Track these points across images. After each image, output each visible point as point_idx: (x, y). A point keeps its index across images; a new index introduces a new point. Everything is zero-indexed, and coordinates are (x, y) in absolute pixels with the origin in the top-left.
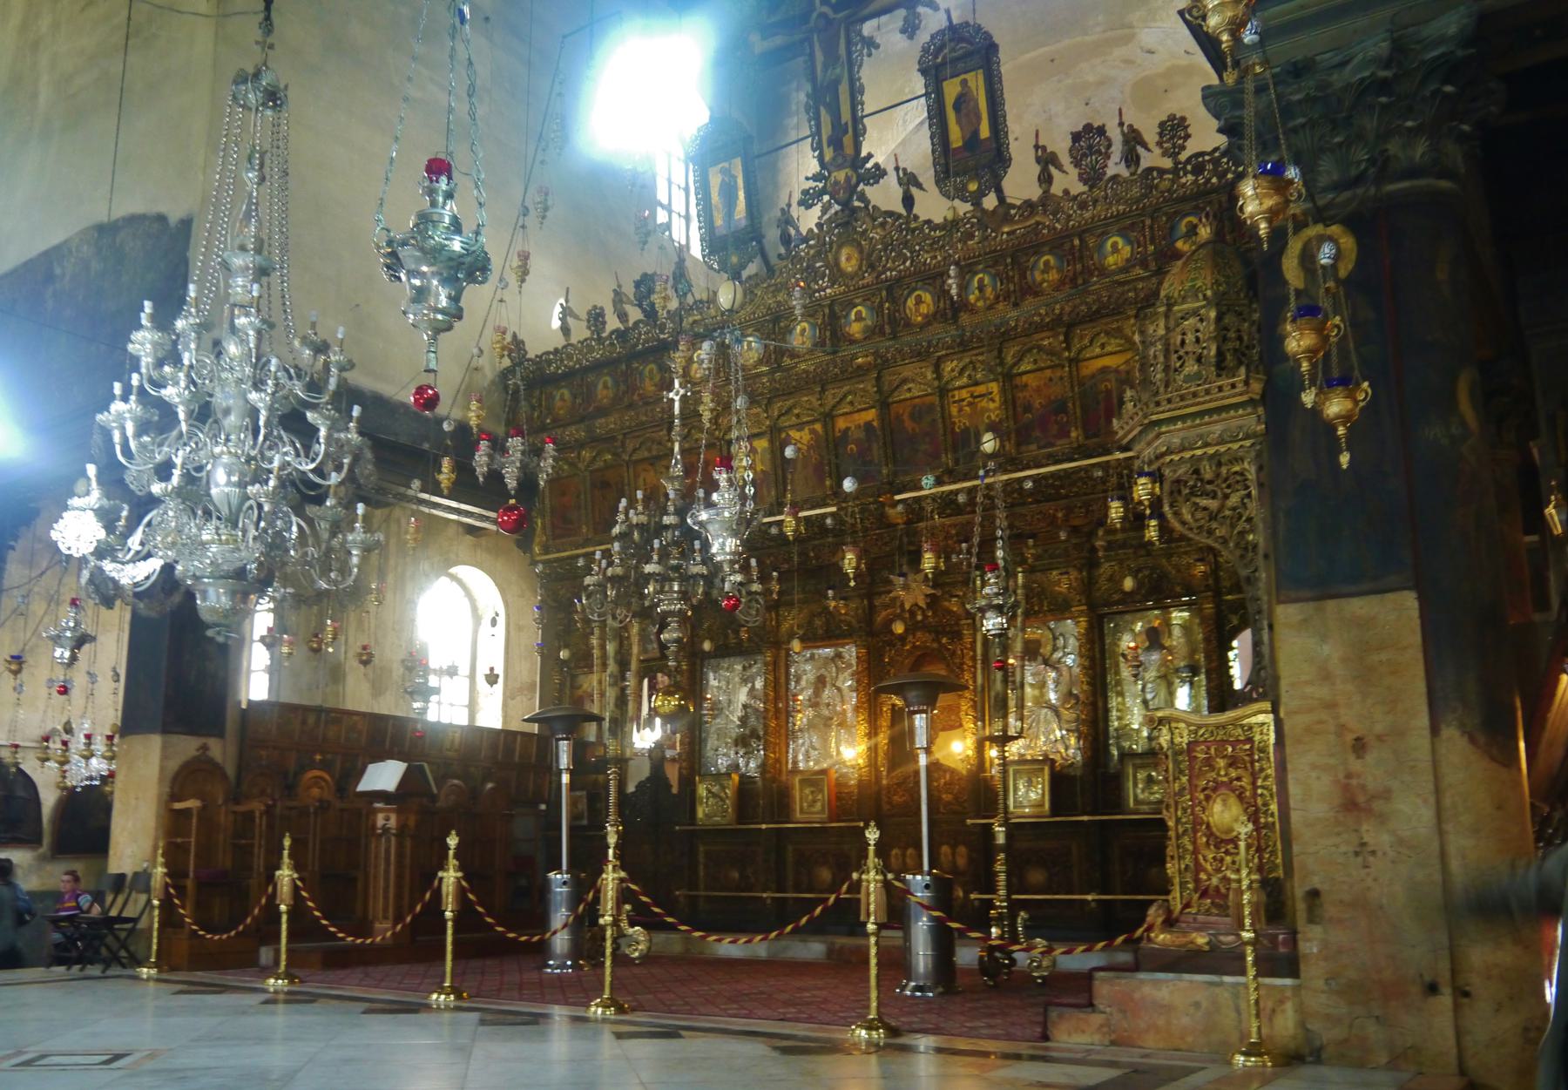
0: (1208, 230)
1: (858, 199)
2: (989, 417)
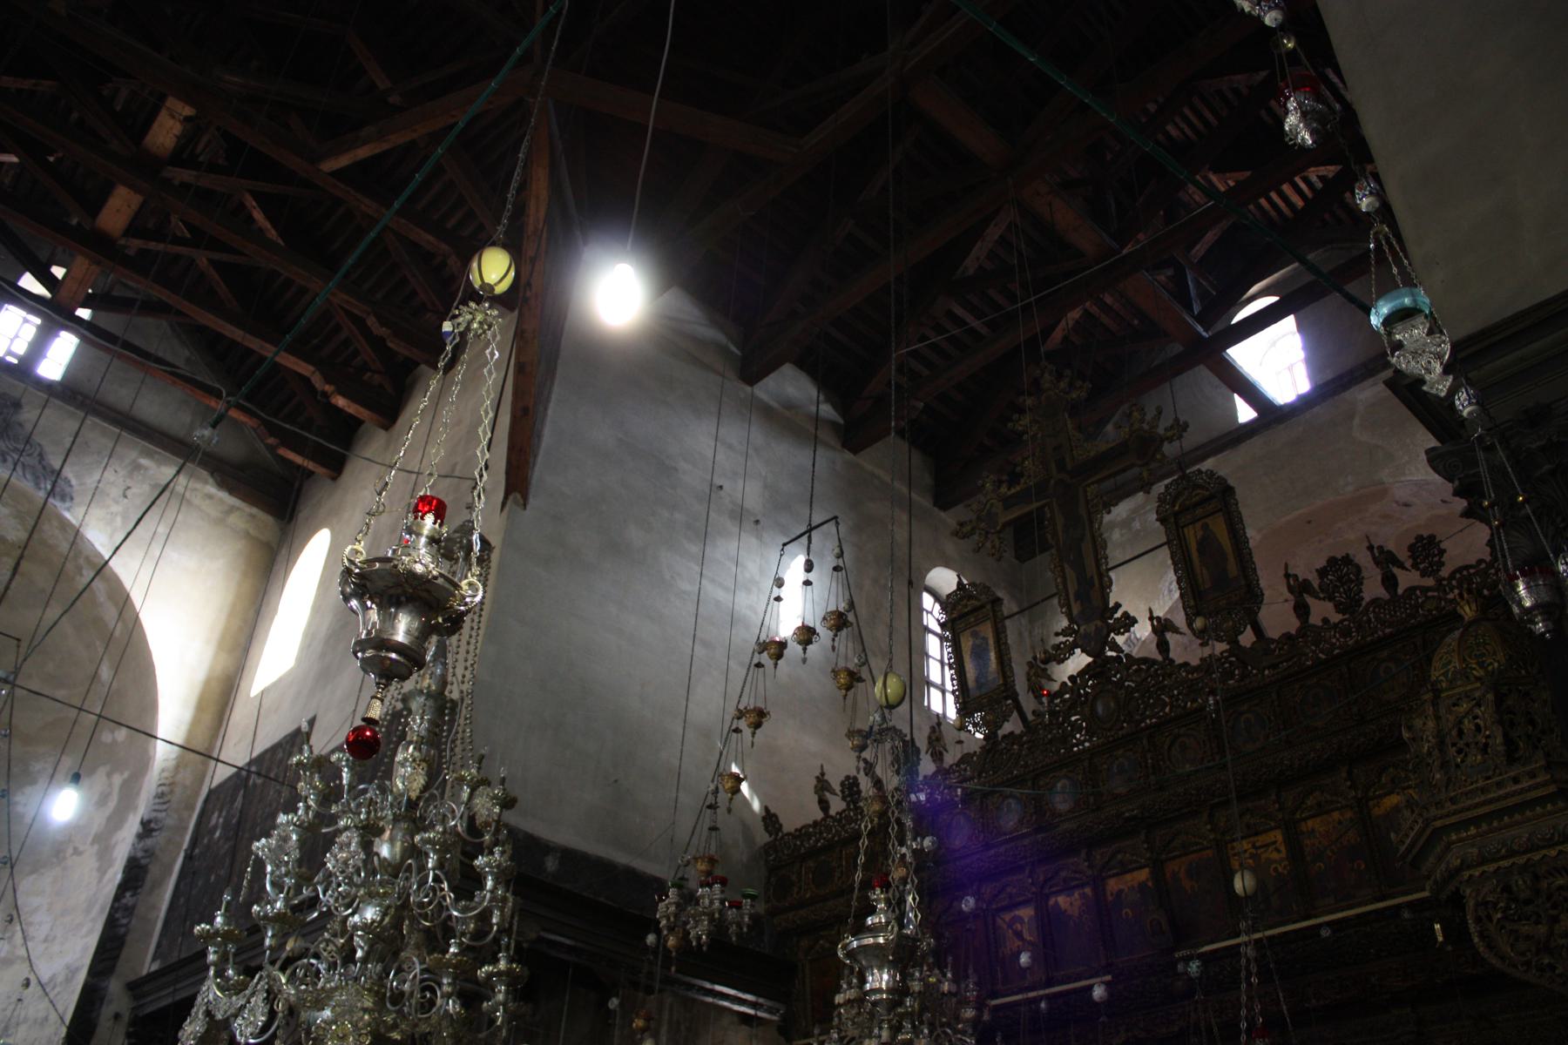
0: (1474, 607)
1: (1111, 650)
2: (1276, 869)
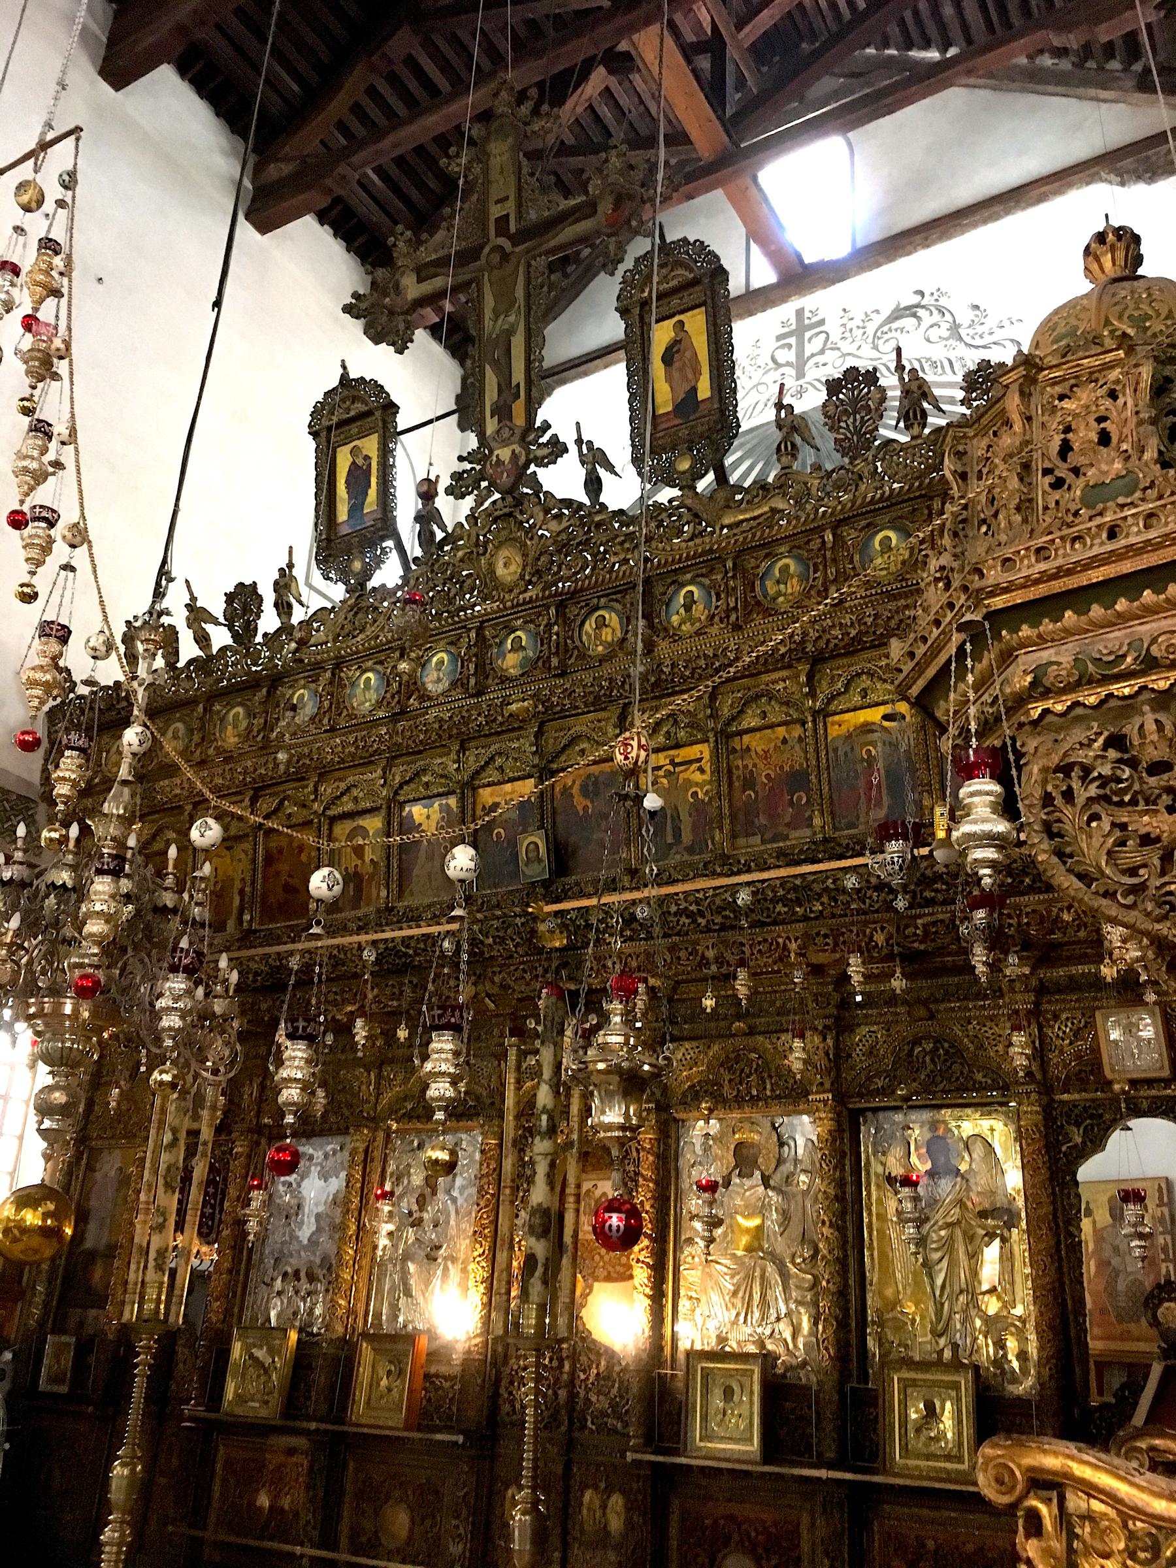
2: (695, 794)
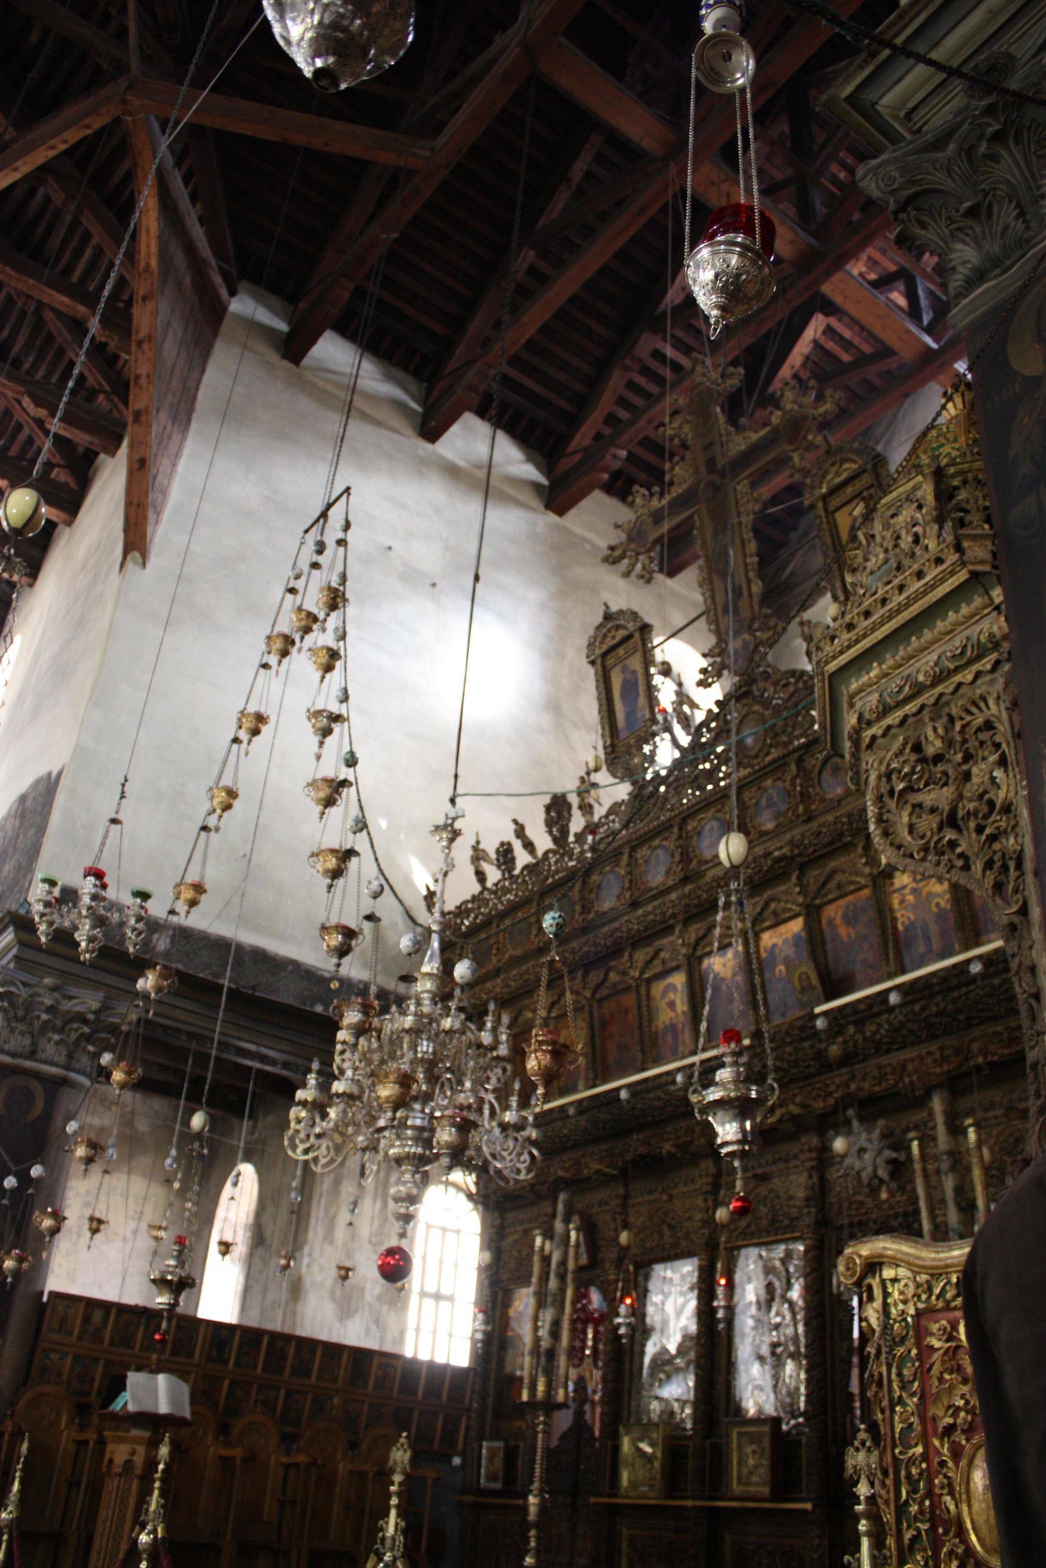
2: (938, 904)
